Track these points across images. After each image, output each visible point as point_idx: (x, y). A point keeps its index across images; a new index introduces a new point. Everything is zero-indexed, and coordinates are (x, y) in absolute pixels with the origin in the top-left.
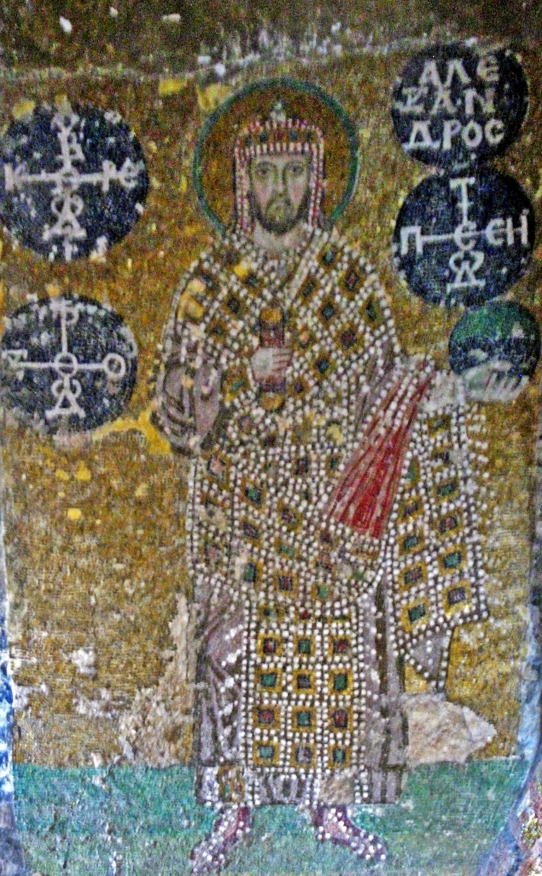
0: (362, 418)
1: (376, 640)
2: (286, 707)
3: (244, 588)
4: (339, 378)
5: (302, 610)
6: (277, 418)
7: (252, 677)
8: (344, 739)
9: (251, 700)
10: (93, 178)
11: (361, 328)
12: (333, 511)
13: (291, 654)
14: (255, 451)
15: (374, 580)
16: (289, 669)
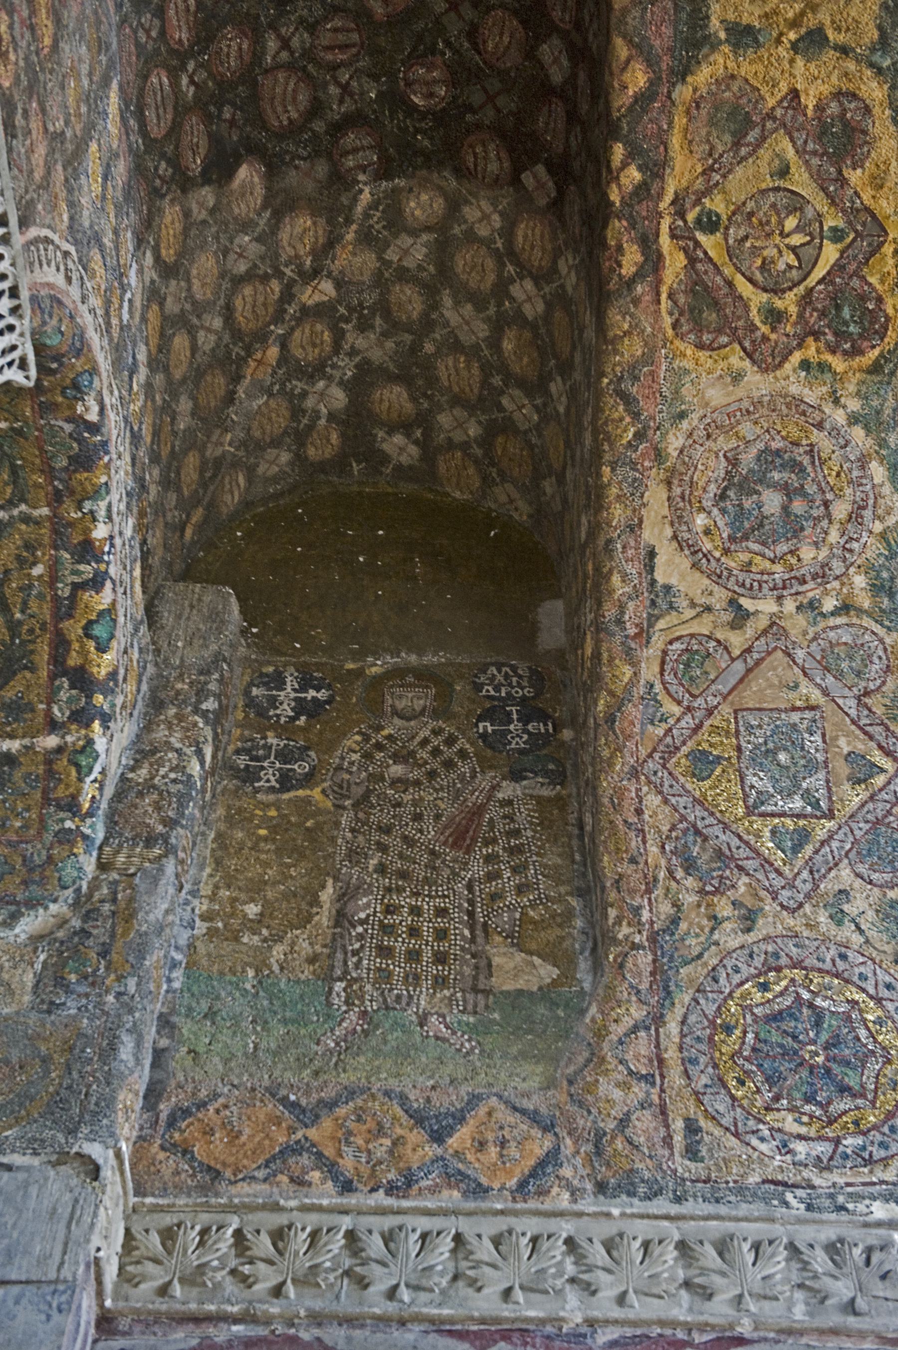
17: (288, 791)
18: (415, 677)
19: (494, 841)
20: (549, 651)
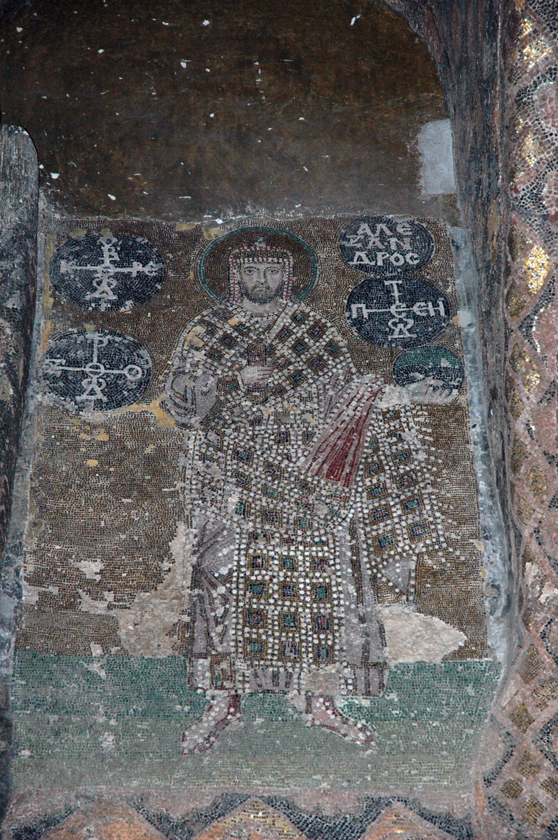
0: (330, 410)
1: (352, 561)
2: (273, 611)
3: (235, 519)
4: (310, 385)
5: (286, 536)
6: (262, 408)
7: (241, 586)
8: (327, 639)
9: (241, 604)
10: (126, 270)
11: (325, 358)
12: (309, 468)
13: (276, 569)
14: (245, 427)
15: (347, 516)
16: (275, 580)
17: (119, 405)
18: (268, 242)
19: (380, 469)
20: (435, 198)
